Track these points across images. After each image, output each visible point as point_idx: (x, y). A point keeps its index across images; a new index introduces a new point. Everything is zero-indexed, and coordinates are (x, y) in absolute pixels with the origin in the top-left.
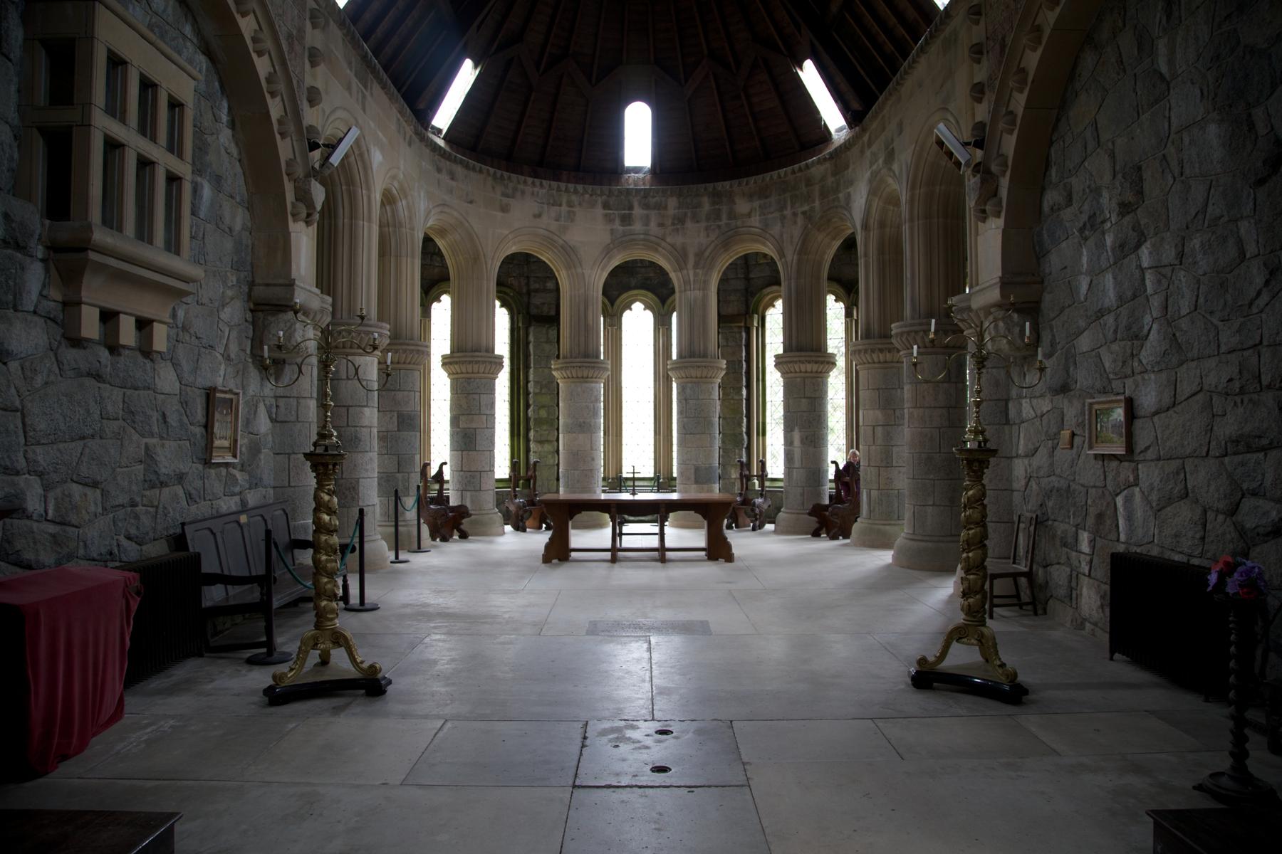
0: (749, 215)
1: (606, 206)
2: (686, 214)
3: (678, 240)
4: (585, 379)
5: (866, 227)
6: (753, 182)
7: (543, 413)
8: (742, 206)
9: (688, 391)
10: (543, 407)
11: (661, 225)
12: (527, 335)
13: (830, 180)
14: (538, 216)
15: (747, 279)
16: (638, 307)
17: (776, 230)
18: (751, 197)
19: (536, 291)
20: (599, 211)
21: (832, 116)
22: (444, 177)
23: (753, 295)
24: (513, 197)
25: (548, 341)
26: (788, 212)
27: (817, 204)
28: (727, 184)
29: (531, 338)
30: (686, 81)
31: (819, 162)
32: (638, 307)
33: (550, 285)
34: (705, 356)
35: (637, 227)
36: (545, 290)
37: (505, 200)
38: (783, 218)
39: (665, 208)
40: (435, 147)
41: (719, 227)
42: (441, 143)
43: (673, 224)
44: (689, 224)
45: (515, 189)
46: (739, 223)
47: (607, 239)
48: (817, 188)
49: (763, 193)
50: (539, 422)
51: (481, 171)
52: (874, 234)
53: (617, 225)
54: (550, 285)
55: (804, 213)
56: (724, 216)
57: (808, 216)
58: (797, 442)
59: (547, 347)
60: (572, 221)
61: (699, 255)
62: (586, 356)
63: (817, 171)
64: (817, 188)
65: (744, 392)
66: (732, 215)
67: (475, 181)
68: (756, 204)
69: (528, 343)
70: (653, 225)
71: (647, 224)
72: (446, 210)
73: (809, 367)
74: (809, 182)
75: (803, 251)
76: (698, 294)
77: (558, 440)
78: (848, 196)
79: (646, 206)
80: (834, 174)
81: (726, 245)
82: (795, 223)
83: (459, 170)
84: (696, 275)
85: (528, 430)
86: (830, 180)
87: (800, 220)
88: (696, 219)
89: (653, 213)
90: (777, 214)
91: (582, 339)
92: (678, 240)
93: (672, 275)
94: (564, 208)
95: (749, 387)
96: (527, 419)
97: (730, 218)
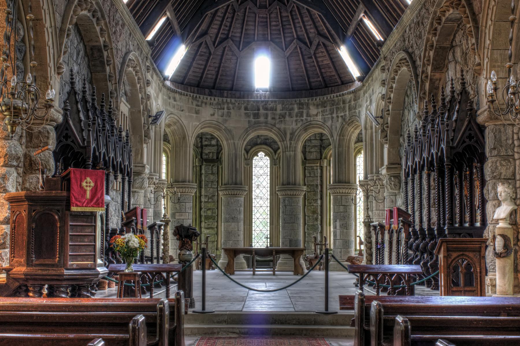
0: (317, 115)
2: (286, 113)
3: (282, 126)
4: (235, 195)
5: (366, 129)
6: (318, 100)
7: (209, 213)
8: (313, 111)
9: (286, 202)
10: (209, 209)
11: (273, 118)
12: (201, 170)
13: (353, 103)
14: (213, 115)
15: (322, 140)
16: (261, 154)
17: (329, 123)
18: (317, 106)
19: (206, 146)
20: (243, 111)
21: (355, 71)
22: (172, 101)
23: (325, 148)
24: (201, 106)
25: (212, 174)
26: (335, 115)
27: (347, 113)
28: (306, 100)
29: (203, 171)
30: (286, 49)
31: (348, 93)
32: (261, 154)
33: (214, 142)
34: (295, 184)
35: (262, 119)
36: (210, 145)
37: (197, 108)
38: (332, 118)
39: (276, 110)
40: (169, 89)
41: (302, 120)
42: (168, 83)
43: (279, 118)
44: (287, 118)
45: (202, 102)
47: (247, 126)
48: (347, 105)
49: (323, 105)
50: (207, 218)
51: (187, 95)
52: (369, 131)
53: (252, 119)
54: (214, 142)
55: (342, 116)
56: (305, 115)
57: (344, 119)
58: (338, 227)
59: (212, 177)
60: (230, 116)
61: (292, 134)
62: (236, 184)
63: (348, 97)
64: (347, 105)
65: (319, 202)
66: (308, 115)
69: (201, 174)
70: (269, 118)
71: (267, 118)
72: (172, 116)
73: (344, 191)
74: (344, 102)
76: (292, 153)
77: (217, 227)
78: (359, 112)
80: (355, 100)
81: (306, 129)
82: (338, 121)
83: (177, 96)
84: (291, 144)
85: (201, 222)
87: (340, 120)
88: (290, 115)
89: (269, 112)
90: (330, 116)
91: (234, 175)
92: (282, 126)
93: (279, 143)
95: (321, 198)
96: (200, 216)
97: (307, 116)
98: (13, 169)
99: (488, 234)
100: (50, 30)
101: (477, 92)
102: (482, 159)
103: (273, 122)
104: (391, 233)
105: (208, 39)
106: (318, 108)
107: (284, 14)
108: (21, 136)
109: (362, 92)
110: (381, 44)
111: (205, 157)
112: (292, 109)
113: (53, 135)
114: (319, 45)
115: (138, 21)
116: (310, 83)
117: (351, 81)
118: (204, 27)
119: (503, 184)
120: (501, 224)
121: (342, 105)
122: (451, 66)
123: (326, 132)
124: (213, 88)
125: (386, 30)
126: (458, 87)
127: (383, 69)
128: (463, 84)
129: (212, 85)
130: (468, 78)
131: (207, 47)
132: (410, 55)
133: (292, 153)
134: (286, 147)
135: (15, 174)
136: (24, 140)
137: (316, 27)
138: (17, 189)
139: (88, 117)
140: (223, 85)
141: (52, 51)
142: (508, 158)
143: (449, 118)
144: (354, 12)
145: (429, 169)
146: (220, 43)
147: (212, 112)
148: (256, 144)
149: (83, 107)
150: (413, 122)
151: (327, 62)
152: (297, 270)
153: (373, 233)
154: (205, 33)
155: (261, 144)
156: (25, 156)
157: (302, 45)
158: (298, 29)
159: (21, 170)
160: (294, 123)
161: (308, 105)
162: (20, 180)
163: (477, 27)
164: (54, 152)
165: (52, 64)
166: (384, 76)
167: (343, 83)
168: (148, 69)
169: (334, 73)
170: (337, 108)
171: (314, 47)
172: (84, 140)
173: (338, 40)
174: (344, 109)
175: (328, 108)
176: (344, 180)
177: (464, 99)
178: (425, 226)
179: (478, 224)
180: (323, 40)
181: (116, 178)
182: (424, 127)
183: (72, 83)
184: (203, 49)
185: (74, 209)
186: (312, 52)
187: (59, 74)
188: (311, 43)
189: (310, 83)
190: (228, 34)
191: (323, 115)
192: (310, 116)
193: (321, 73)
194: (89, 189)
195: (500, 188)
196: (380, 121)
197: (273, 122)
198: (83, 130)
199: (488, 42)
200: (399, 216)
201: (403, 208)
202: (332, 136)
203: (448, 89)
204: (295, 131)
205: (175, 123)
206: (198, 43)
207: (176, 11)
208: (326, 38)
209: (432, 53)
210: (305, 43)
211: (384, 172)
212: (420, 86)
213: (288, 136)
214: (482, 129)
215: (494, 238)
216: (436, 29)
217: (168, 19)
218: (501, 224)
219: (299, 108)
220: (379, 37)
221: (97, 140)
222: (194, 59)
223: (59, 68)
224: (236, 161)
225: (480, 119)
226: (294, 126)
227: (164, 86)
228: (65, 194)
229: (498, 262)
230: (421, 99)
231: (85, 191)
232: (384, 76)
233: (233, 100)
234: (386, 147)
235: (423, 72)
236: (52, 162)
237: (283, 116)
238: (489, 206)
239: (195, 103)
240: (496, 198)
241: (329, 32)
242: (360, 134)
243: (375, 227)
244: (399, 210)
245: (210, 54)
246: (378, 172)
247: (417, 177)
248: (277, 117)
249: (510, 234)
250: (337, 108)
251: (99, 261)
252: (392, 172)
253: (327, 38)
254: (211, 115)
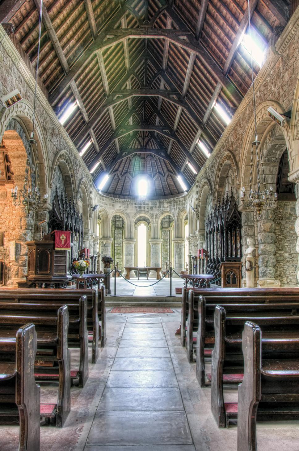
3: (152, 212)
4: (130, 243)
5: (189, 213)
6: (168, 200)
7: (119, 251)
8: (166, 205)
11: (148, 209)
13: (183, 202)
15: (169, 218)
17: (173, 211)
19: (117, 221)
20: (134, 205)
22: (102, 200)
23: (171, 222)
25: (120, 234)
26: (175, 207)
29: (116, 233)
33: (121, 219)
35: (142, 209)
36: (119, 221)
38: (174, 208)
40: (100, 195)
44: (154, 208)
47: (136, 212)
49: (170, 202)
50: (118, 254)
52: (191, 215)
53: (138, 209)
54: (121, 219)
56: (162, 207)
57: (179, 209)
59: (120, 235)
61: (156, 216)
62: (131, 238)
63: (181, 199)
65: (168, 246)
66: (164, 207)
67: (107, 201)
68: (169, 205)
69: (115, 234)
73: (179, 241)
74: (180, 201)
75: (178, 216)
76: (156, 224)
80: (184, 200)
81: (162, 213)
83: (104, 198)
85: (115, 255)
86: (183, 202)
87: (178, 209)
88: (155, 207)
89: (146, 206)
92: (152, 212)
95: (169, 245)
96: (115, 253)
98: (29, 231)
99: (243, 260)
100: (47, 168)
101: (238, 197)
102: (240, 227)
104: (200, 260)
105: (118, 173)
107: (153, 162)
108: (33, 216)
109: (187, 197)
110: (196, 175)
111: (116, 226)
112: (156, 204)
113: (48, 215)
114: (168, 176)
115: (87, 164)
116: (164, 192)
117: (183, 192)
118: (116, 167)
119: (250, 238)
120: (249, 256)
121: (178, 203)
122: (227, 185)
123: (171, 215)
124: (121, 195)
125: (199, 169)
126: (230, 195)
127: (197, 187)
128: (232, 193)
129: (120, 193)
130: (234, 191)
131: (118, 176)
132: (209, 180)
133: (156, 224)
134: (153, 222)
135: (30, 233)
136: (34, 218)
137: (167, 168)
138: (31, 240)
139: (63, 207)
140: (125, 194)
141: (47, 177)
142: (252, 227)
143: (226, 208)
144: (184, 161)
145: (217, 232)
146: (123, 175)
147: (120, 206)
148: (140, 220)
149: (61, 203)
150: (210, 210)
151: (172, 183)
152: (158, 278)
153: (192, 260)
154: (117, 170)
155: (142, 220)
156: (35, 225)
157: (161, 176)
158: (159, 168)
159: (33, 231)
161: (163, 203)
162: (33, 236)
163: (238, 168)
164: (48, 223)
165: (47, 183)
166: (197, 190)
167: (179, 193)
168: (91, 186)
169: (175, 188)
170: (177, 204)
171: (166, 176)
172: (61, 218)
173: (177, 173)
175: (172, 204)
176: (179, 237)
177: (232, 199)
178: (215, 257)
179: (239, 256)
180: (170, 173)
181: (76, 235)
182: (215, 212)
183: (57, 192)
184: (116, 177)
185: (56, 249)
186: (165, 179)
187: (50, 188)
188: (165, 175)
189: (164, 192)
190: (127, 170)
193: (169, 188)
194: (63, 240)
195: (248, 240)
196: (196, 210)
197: (147, 210)
198: (61, 213)
199: (242, 175)
200: (203, 252)
201: (206, 249)
202: (174, 217)
203: (226, 196)
205: (103, 211)
206: (114, 174)
207: (104, 160)
208: (172, 172)
209: (218, 180)
210: (162, 175)
211: (197, 233)
212: (213, 194)
213: (154, 217)
214: (240, 213)
215: (246, 262)
216: (220, 169)
217: (100, 163)
218: (249, 256)
220: (195, 172)
221: (67, 218)
222: (112, 182)
223: (51, 185)
225: (240, 209)
226: (157, 212)
227: (98, 193)
228: (52, 242)
229: (247, 273)
230: (214, 200)
231: (62, 241)
232: (197, 190)
233: (129, 200)
234: (198, 222)
235: (214, 188)
236: (47, 228)
237: (152, 208)
238: (244, 248)
239: (112, 201)
240: (246, 244)
241: (173, 170)
242: (187, 216)
243: (193, 258)
244: (203, 250)
245: (119, 179)
246: (195, 233)
247: (212, 235)
248: (149, 208)
249: (253, 261)
250: (177, 204)
251: (68, 273)
252: (202, 233)
253: (172, 172)
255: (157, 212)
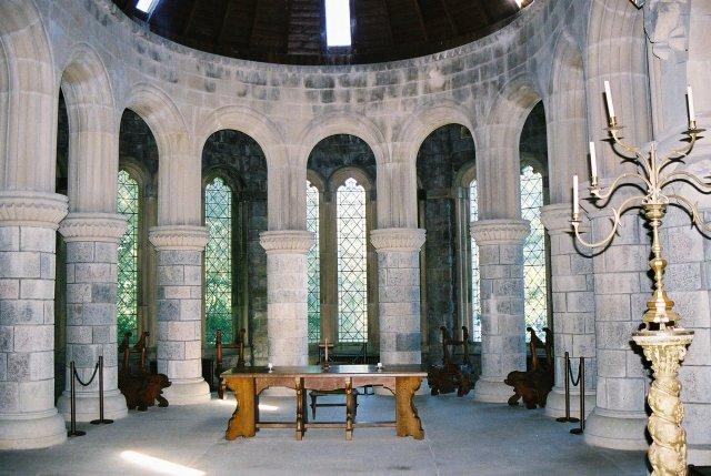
1: (309, 84)
2: (384, 89)
3: (378, 115)
11: (360, 100)
16: (351, 182)
20: (302, 89)
26: (479, 83)
27: (506, 73)
32: (351, 182)
35: (338, 103)
37: (210, 79)
39: (365, 84)
41: (415, 101)
43: (372, 100)
44: (387, 99)
46: (434, 95)
48: (505, 57)
55: (494, 83)
56: (420, 89)
58: (493, 309)
60: (276, 99)
68: (450, 76)
70: (353, 100)
71: (348, 100)
79: (346, 83)
84: (394, 147)
88: (393, 93)
89: (353, 90)
94: (269, 87)
103: (360, 107)
106: (445, 74)
112: (395, 81)
160: (400, 108)
174: (499, 68)
191: (455, 86)
192: (430, 91)
204: (404, 121)
213: (389, 133)
219: (410, 78)
224: (290, 183)
226: (400, 113)
237: (379, 95)
248: (368, 97)
254: (240, 95)
255: (400, 113)
